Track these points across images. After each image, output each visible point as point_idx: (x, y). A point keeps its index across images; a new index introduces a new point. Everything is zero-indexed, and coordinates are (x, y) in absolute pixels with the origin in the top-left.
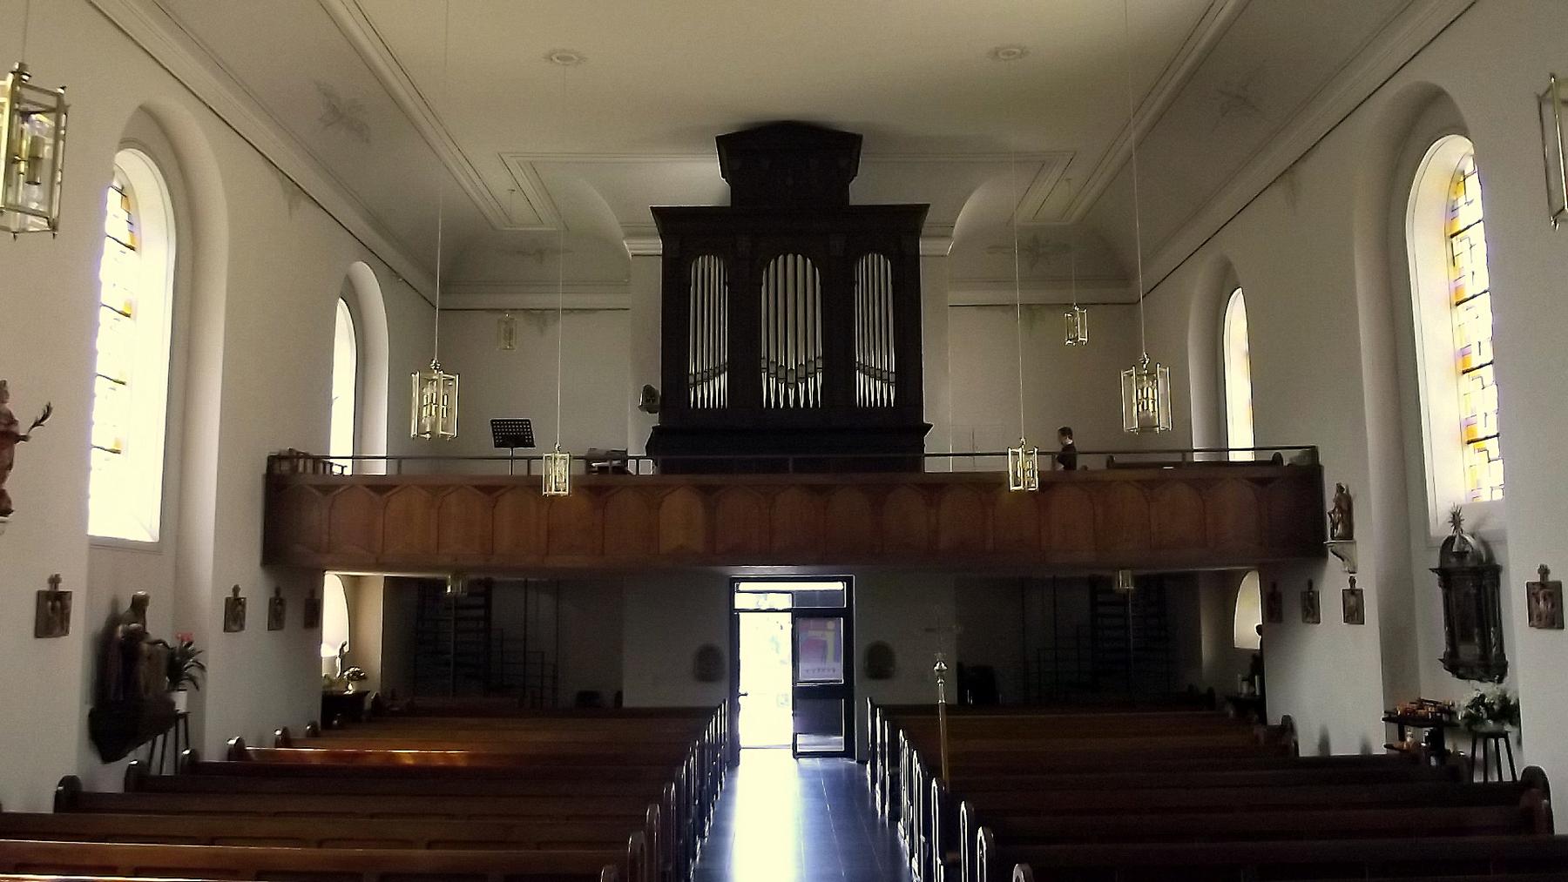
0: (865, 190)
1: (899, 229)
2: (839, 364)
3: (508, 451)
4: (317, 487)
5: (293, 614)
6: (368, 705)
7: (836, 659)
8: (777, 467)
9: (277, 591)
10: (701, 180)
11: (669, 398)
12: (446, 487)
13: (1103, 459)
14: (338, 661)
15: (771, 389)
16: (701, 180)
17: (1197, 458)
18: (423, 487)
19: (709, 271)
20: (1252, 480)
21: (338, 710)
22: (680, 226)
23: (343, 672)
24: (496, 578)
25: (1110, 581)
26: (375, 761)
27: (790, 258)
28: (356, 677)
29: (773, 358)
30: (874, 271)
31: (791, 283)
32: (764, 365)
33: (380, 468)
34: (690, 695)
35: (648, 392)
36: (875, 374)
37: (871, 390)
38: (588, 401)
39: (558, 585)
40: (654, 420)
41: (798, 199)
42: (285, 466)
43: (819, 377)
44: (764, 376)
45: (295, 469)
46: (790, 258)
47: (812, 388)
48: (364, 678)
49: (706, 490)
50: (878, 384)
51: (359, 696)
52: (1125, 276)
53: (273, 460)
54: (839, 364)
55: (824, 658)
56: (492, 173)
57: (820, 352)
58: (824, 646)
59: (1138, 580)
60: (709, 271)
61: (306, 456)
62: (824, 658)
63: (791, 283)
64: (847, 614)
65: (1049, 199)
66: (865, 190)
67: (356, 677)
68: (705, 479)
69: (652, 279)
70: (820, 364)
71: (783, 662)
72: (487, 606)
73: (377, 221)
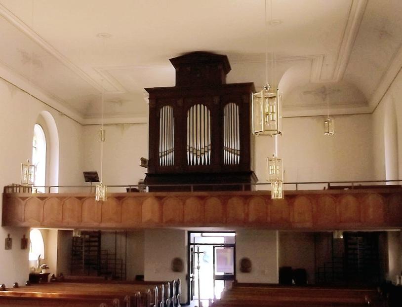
0: (233, 77)
1: (242, 94)
2: (217, 145)
3: (89, 183)
4: (21, 198)
5: (16, 244)
6: (50, 276)
7: (231, 265)
8: (188, 189)
9: (9, 235)
10: (167, 77)
11: (152, 162)
12: (65, 197)
13: (326, 185)
14: (38, 262)
15: (191, 158)
16: (167, 77)
17: (388, 184)
18: (57, 197)
19: (167, 112)
20: (332, 195)
21: (35, 279)
22: (158, 96)
23: (39, 266)
24: (102, 231)
25: (332, 234)
26: (27, 296)
27: (199, 106)
28: (45, 267)
29: (191, 146)
30: (232, 112)
31: (199, 118)
32: (188, 148)
33: (56, 191)
34: (173, 277)
35: (143, 161)
36: (231, 151)
37: (231, 157)
38: (125, 161)
39: (127, 233)
40: (146, 170)
41: (205, 82)
42: (10, 190)
43: (210, 152)
44: (188, 153)
45: (13, 190)
46: (199, 106)
47: (206, 158)
48: (48, 268)
49: (159, 198)
50: (233, 155)
51: (46, 275)
52: (366, 102)
53: (6, 188)
54: (217, 145)
55: (226, 264)
56: (95, 75)
57: (210, 143)
58: (226, 259)
59: (345, 234)
60: (167, 112)
61: (20, 186)
62: (226, 264)
63: (199, 118)
64: (233, 246)
65: (326, 71)
66: (233, 77)
67: (45, 267)
68: (159, 194)
69: (145, 118)
70: (210, 147)
71: (231, 265)
72: (99, 242)
73: (54, 97)
